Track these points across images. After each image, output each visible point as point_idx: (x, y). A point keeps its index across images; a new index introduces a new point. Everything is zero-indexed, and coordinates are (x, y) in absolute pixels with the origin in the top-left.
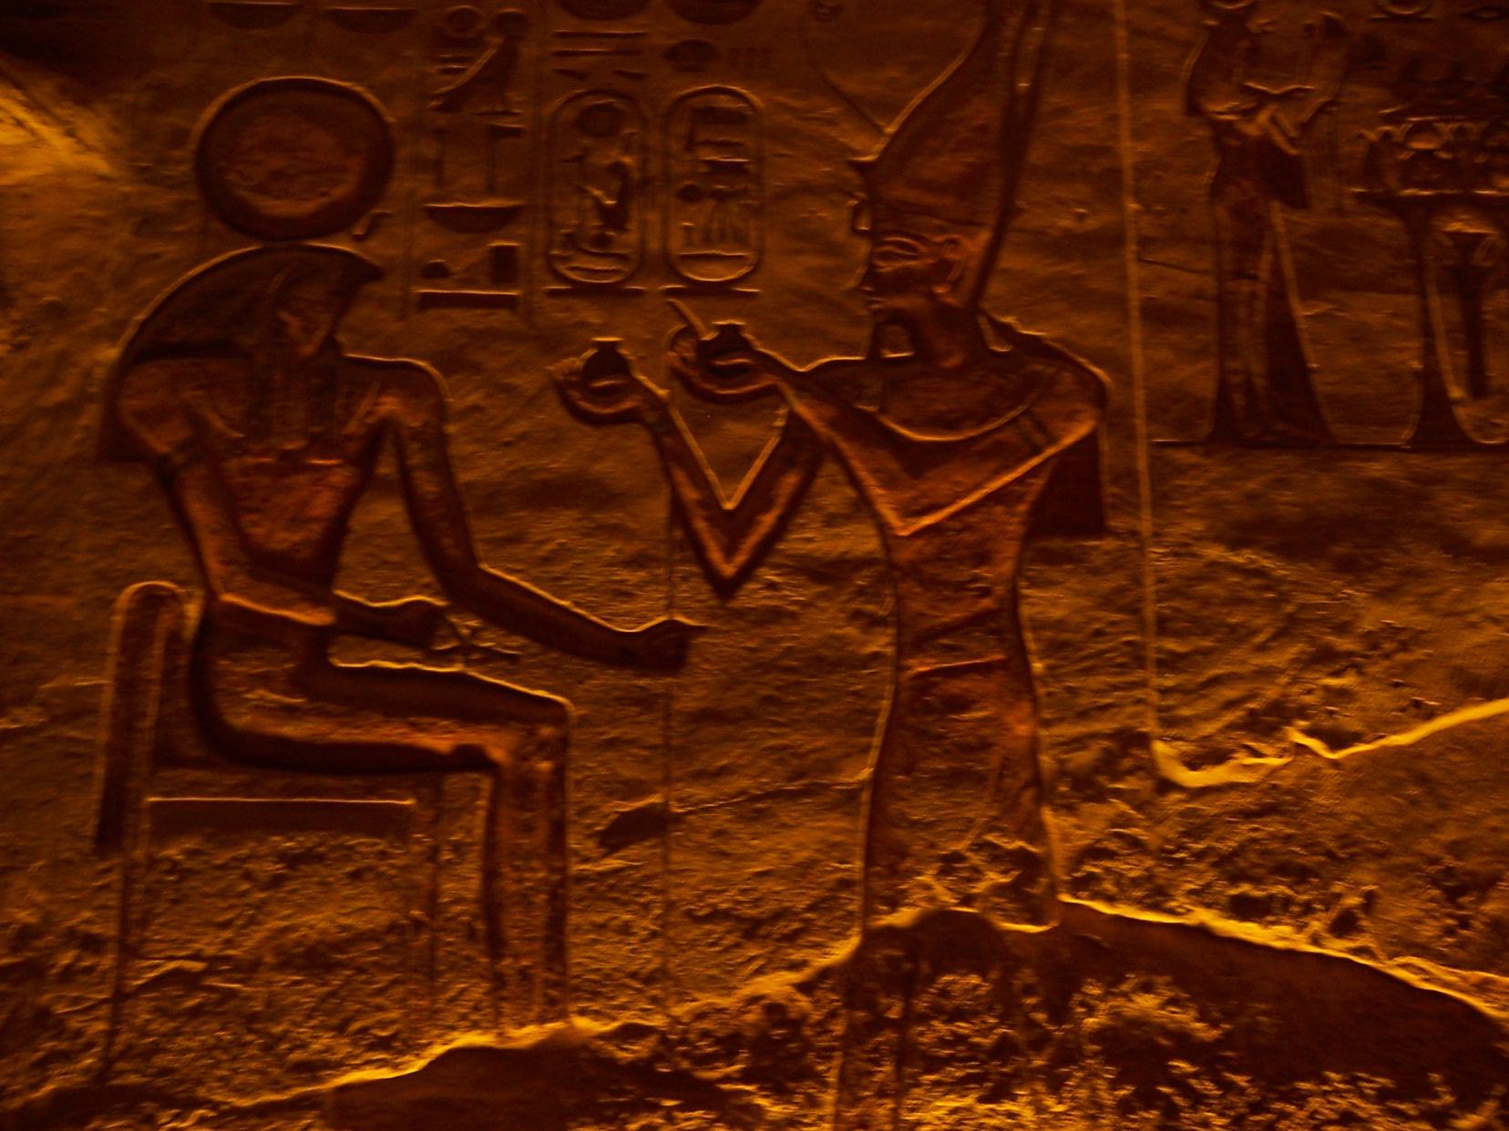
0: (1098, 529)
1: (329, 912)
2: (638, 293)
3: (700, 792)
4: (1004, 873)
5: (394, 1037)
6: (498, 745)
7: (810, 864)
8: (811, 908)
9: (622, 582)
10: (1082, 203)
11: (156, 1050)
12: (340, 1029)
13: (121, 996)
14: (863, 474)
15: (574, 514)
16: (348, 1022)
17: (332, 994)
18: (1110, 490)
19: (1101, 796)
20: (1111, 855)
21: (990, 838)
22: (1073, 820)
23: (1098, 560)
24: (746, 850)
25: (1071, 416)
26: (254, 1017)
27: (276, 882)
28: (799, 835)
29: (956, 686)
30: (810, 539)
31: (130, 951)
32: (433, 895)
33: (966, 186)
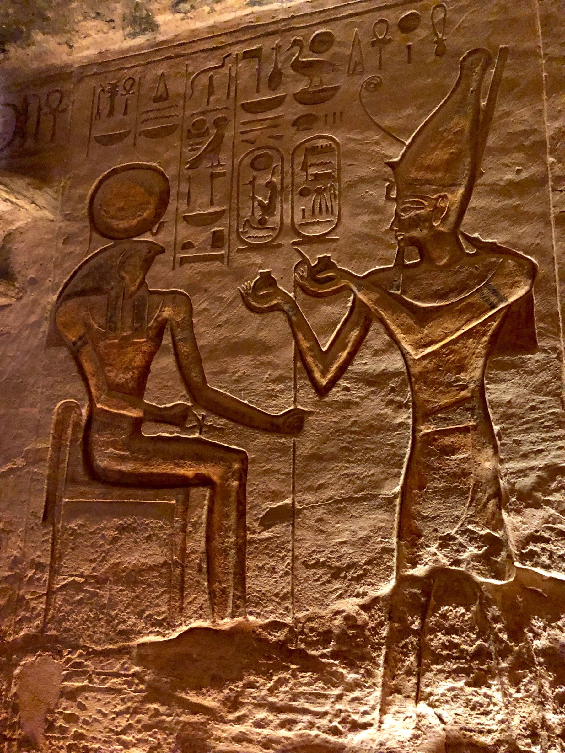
0: (532, 348)
1: (136, 555)
2: (280, 246)
3: (310, 498)
4: (479, 548)
5: (163, 620)
6: (213, 471)
7: (367, 539)
8: (367, 563)
9: (273, 390)
10: (518, 165)
11: (64, 619)
12: (140, 615)
13: (50, 593)
14: (393, 328)
15: (250, 357)
16: (143, 611)
17: (137, 597)
18: (539, 325)
19: (537, 505)
20: (547, 541)
21: (470, 527)
22: (520, 518)
23: (531, 366)
24: (333, 529)
25: (514, 285)
26: (104, 606)
27: (115, 540)
28: (361, 522)
29: (448, 440)
30: (366, 363)
31: (54, 571)
32: (184, 549)
33: (450, 165)
